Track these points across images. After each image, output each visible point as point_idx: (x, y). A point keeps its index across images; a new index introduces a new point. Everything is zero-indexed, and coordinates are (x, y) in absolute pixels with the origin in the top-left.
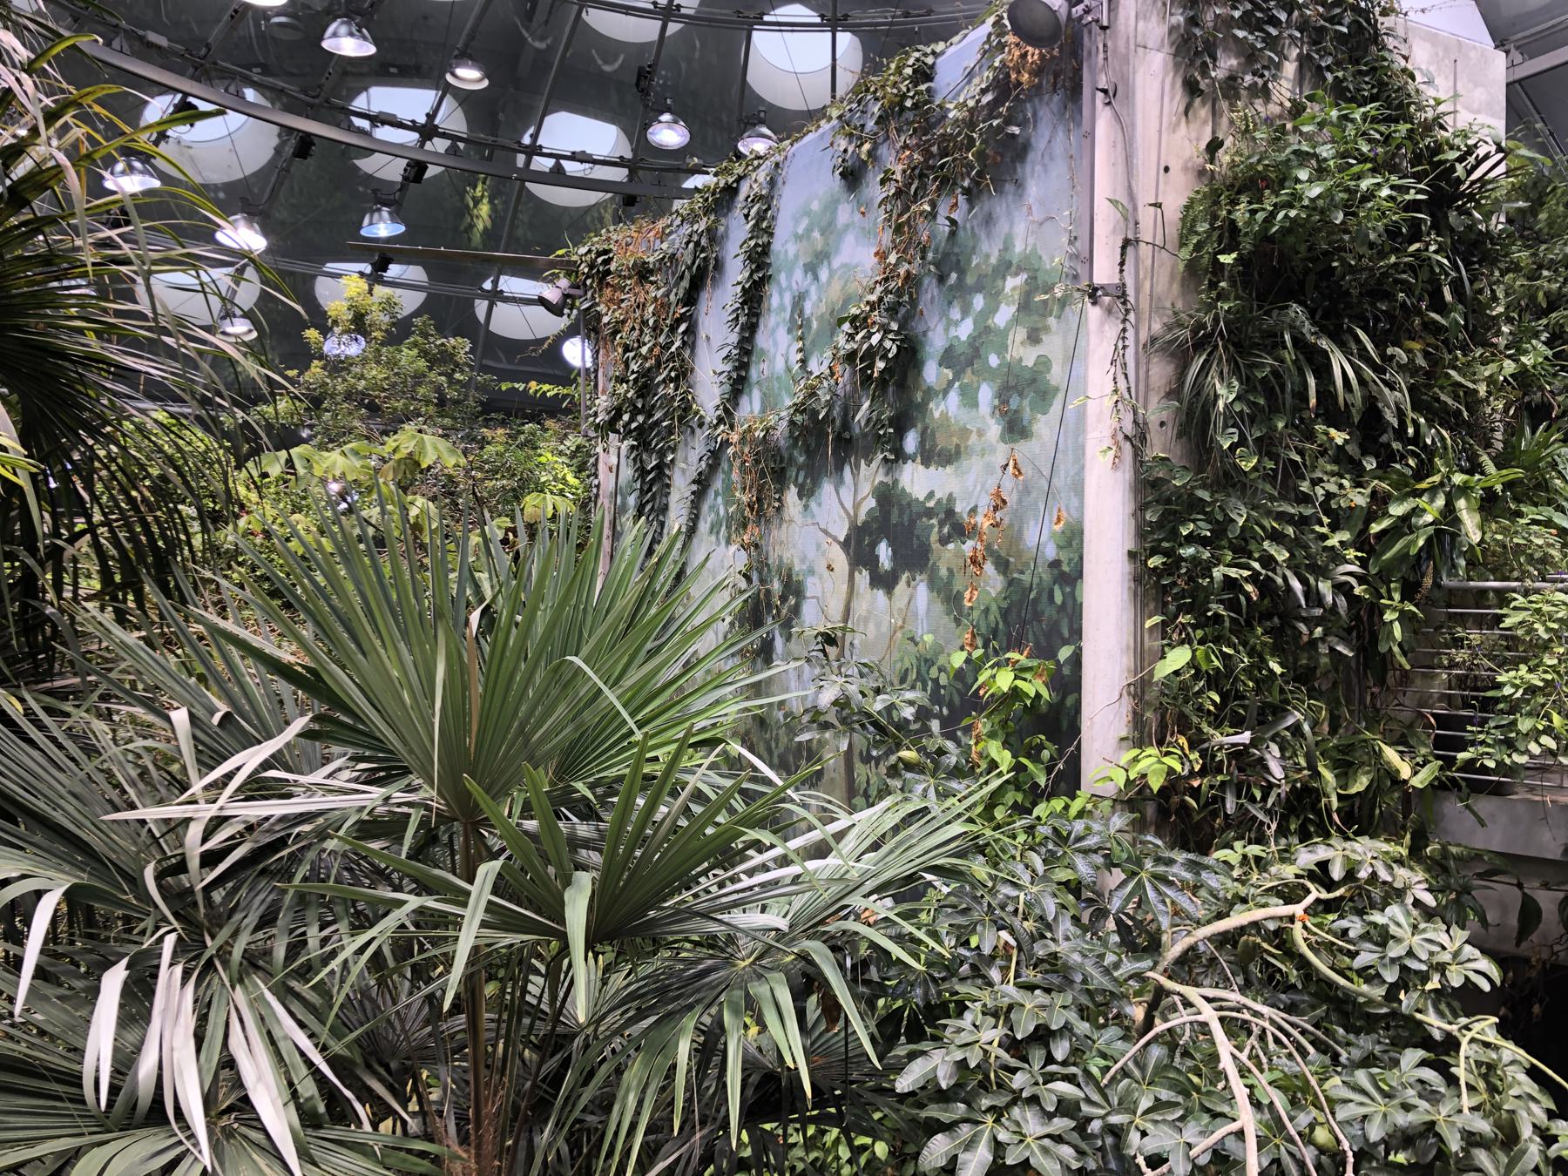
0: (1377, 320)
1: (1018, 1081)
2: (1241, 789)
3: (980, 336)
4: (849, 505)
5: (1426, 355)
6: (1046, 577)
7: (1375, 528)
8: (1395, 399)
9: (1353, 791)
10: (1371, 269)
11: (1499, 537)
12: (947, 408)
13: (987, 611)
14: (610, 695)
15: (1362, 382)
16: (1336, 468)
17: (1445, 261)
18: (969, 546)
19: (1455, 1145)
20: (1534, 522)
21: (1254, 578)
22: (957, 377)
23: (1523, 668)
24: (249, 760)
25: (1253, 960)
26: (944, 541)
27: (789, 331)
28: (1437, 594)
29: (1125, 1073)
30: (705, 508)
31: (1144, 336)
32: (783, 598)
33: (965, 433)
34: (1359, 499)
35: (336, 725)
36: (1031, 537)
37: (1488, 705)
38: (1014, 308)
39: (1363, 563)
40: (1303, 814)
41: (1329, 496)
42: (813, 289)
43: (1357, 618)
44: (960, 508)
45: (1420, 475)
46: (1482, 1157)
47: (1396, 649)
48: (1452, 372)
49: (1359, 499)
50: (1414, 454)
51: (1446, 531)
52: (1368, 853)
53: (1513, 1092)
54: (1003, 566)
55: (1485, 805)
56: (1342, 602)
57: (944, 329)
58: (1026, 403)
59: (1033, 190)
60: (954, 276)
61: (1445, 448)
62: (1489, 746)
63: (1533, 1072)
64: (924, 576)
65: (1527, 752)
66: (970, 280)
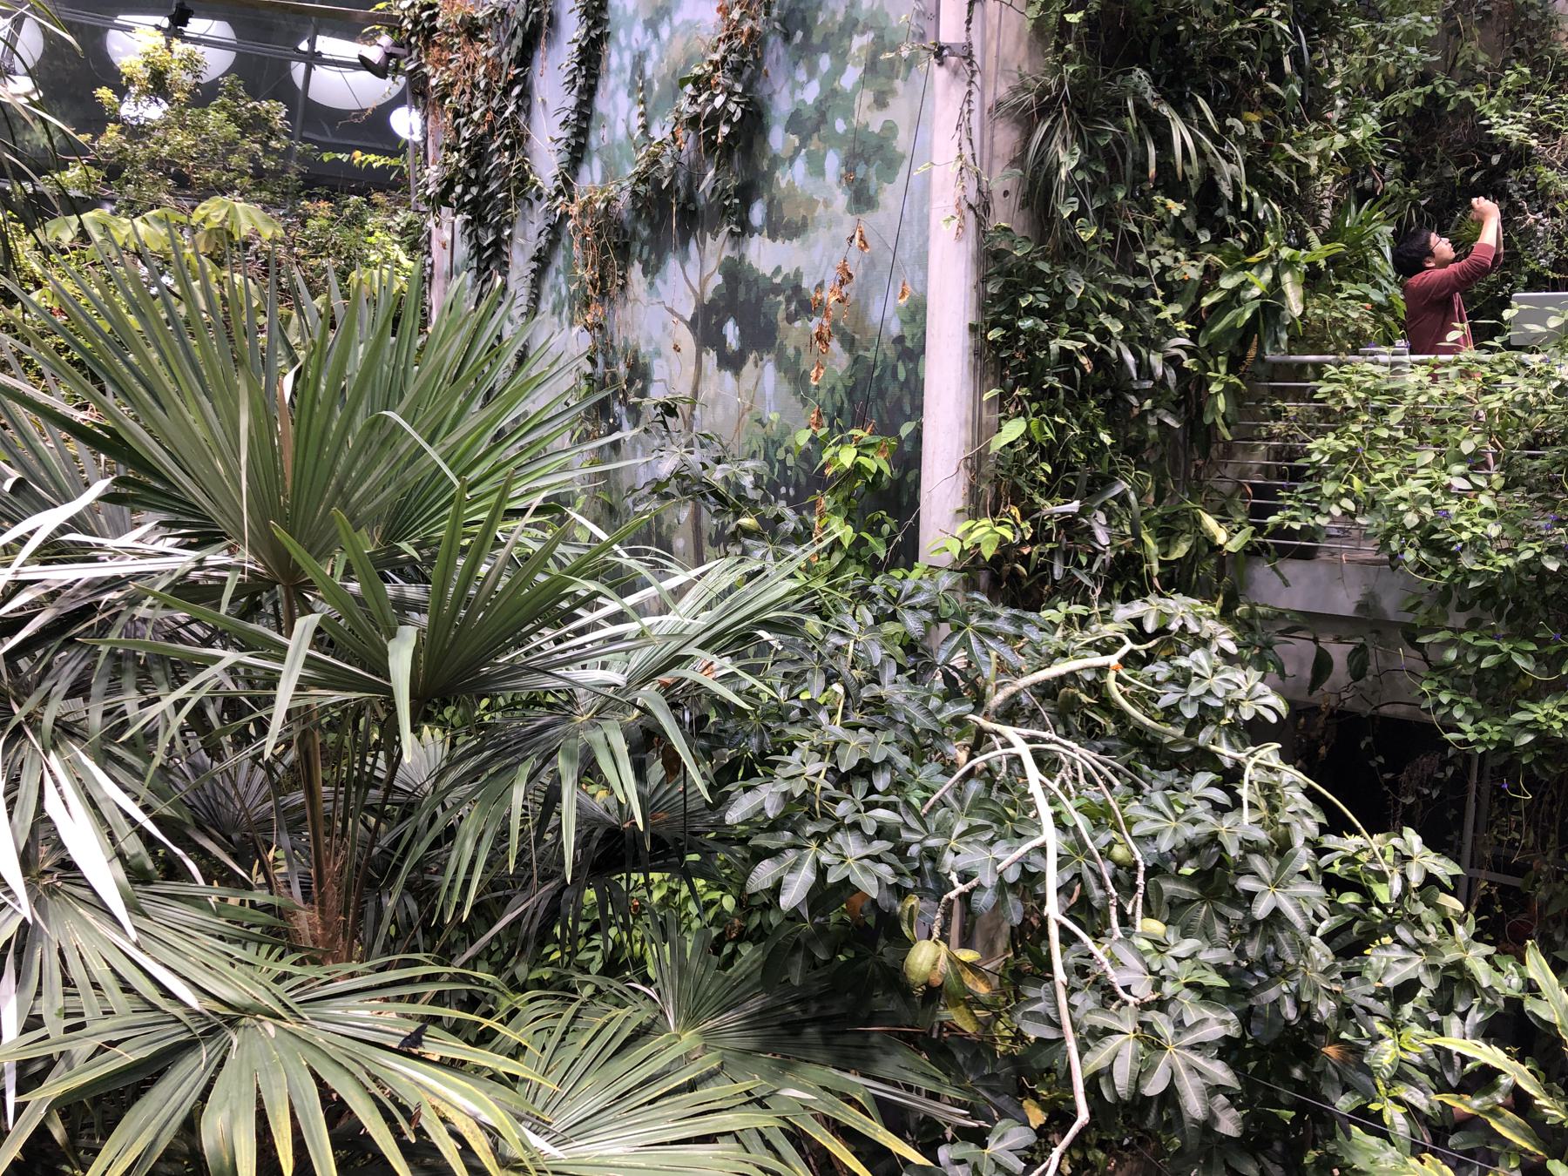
0: (1219, 90)
1: (841, 810)
2: (1069, 556)
3: (826, 99)
4: (695, 282)
5: (1264, 128)
6: (891, 353)
7: (1206, 301)
8: (1231, 172)
9: (1173, 557)
10: (1215, 35)
11: (1319, 311)
12: (793, 177)
13: (833, 389)
14: (433, 453)
15: (1201, 154)
16: (1172, 241)
17: (1286, 28)
18: (814, 325)
19: (1234, 851)
20: (1351, 297)
21: (1089, 350)
22: (803, 144)
23: (1331, 435)
24: (45, 522)
25: (1070, 706)
26: (791, 319)
27: (630, 94)
28: (1260, 368)
29: (942, 803)
30: (546, 287)
31: (989, 101)
32: (630, 382)
33: (811, 203)
34: (1193, 272)
35: (141, 487)
36: (875, 314)
37: (1297, 474)
38: (860, 70)
39: (1193, 335)
40: (1126, 577)
41: (1165, 269)
42: (654, 48)
43: (1185, 391)
44: (807, 283)
45: (1251, 249)
46: (1257, 862)
47: (1220, 421)
48: (1287, 146)
49: (1193, 272)
50: (1247, 229)
51: (1271, 307)
52: (1181, 609)
53: (1289, 809)
54: (849, 343)
55: (1291, 568)
56: (1172, 375)
57: (792, 91)
58: (872, 171)
60: (799, 34)
61: (1275, 223)
62: (1296, 509)
63: (1309, 793)
64: (772, 356)
65: (1329, 514)
66: (816, 39)
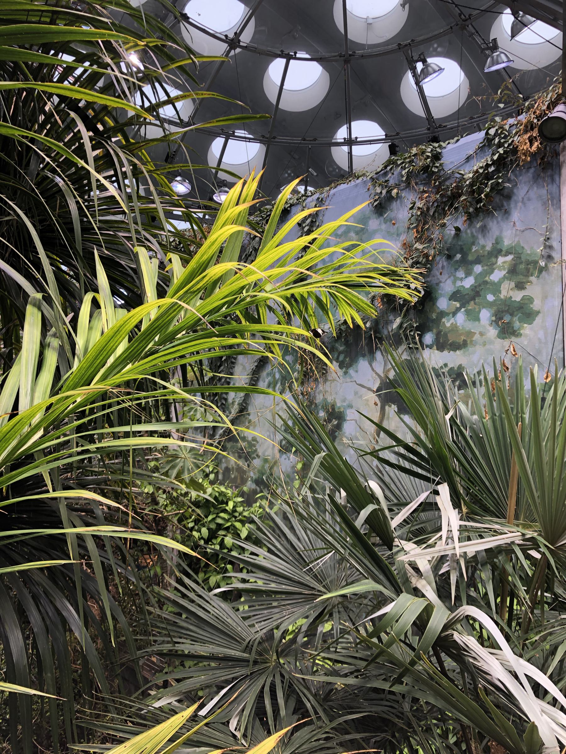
3: (480, 285)
38: (504, 273)
59: (516, 215)
60: (459, 256)
66: (470, 258)
